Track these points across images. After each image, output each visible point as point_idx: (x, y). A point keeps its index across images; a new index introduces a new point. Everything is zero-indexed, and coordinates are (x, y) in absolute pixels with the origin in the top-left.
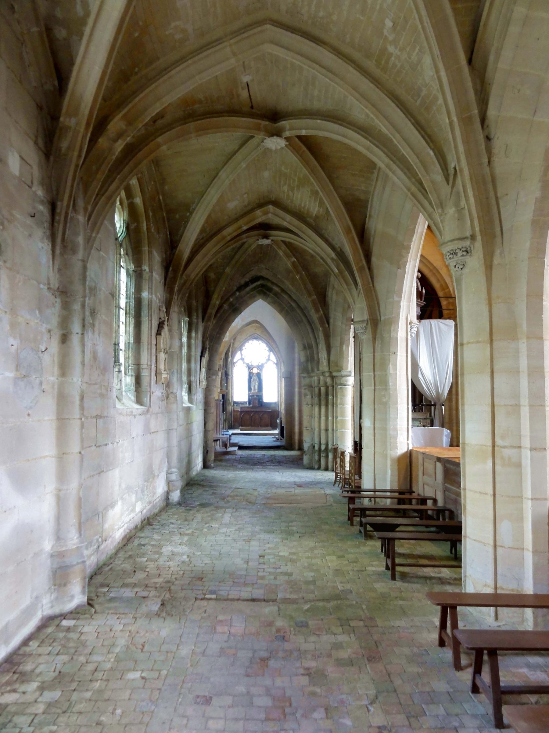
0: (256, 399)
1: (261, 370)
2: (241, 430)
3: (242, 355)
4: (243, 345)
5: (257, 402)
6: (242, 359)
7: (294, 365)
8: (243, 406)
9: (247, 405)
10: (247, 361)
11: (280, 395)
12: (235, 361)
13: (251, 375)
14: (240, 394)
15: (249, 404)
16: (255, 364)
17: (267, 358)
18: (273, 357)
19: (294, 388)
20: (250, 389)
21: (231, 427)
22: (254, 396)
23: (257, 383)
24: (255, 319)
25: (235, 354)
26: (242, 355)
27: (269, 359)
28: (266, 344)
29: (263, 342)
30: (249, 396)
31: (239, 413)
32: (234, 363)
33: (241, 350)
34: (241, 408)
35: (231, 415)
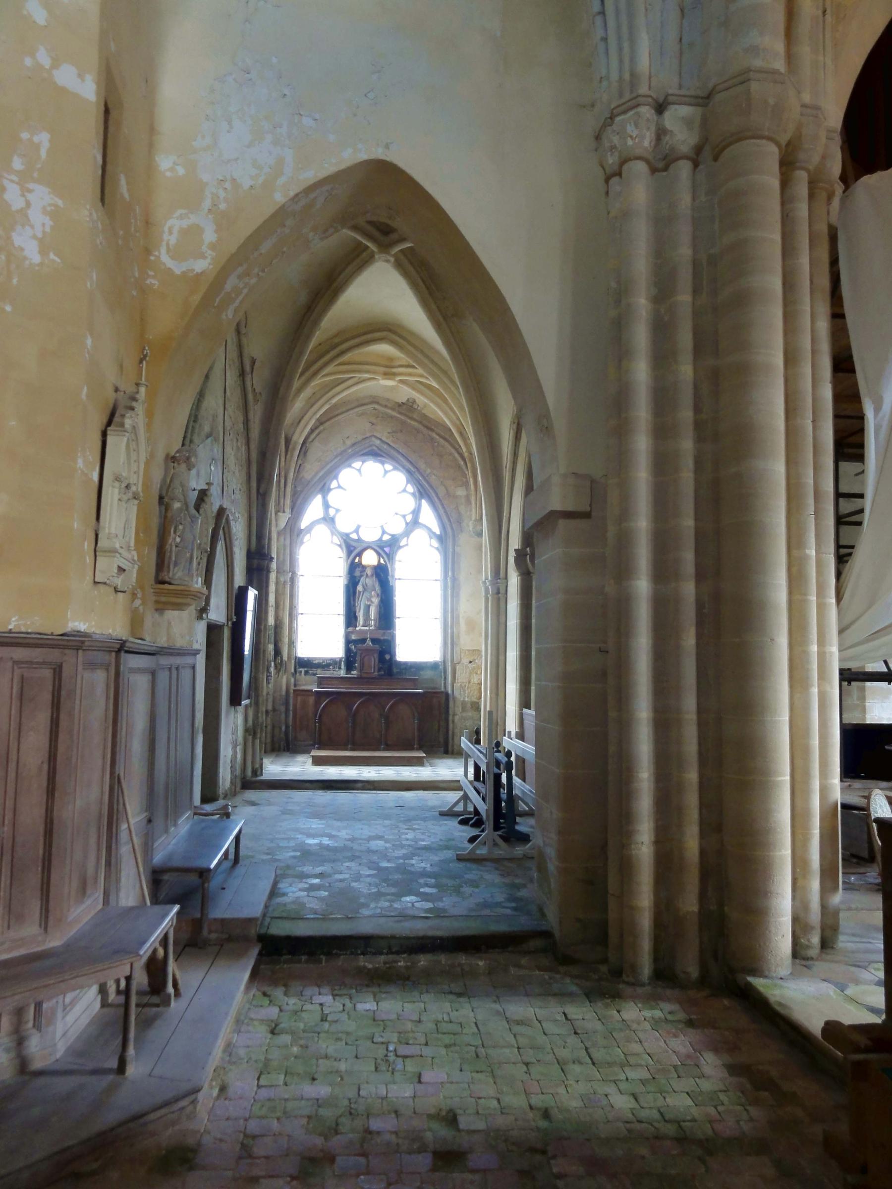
0: (371, 650)
1: (390, 557)
2: (317, 761)
3: (327, 506)
4: (331, 473)
5: (373, 660)
6: (328, 520)
7: (621, 430)
8: (327, 674)
9: (342, 673)
10: (345, 525)
11: (450, 640)
12: (304, 523)
13: (357, 573)
14: (319, 633)
15: (349, 667)
16: (370, 535)
17: (409, 518)
18: (428, 516)
19: (623, 571)
20: (351, 618)
21: (285, 746)
22: (364, 641)
23: (376, 601)
24: (379, 153)
25: (306, 500)
26: (327, 506)
27: (414, 523)
28: (409, 472)
29: (399, 466)
30: (348, 642)
31: (311, 700)
32: (301, 531)
33: (325, 490)
34: (321, 681)
35: (287, 703)
